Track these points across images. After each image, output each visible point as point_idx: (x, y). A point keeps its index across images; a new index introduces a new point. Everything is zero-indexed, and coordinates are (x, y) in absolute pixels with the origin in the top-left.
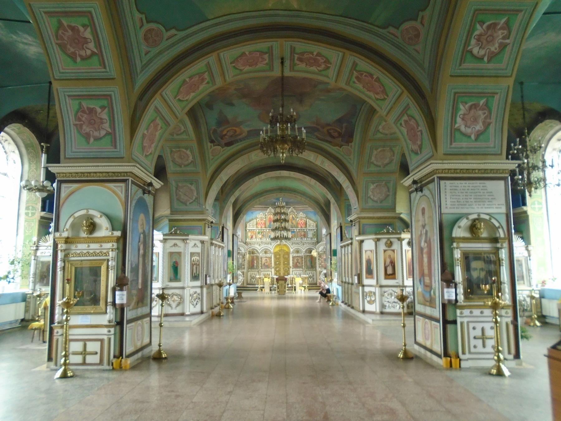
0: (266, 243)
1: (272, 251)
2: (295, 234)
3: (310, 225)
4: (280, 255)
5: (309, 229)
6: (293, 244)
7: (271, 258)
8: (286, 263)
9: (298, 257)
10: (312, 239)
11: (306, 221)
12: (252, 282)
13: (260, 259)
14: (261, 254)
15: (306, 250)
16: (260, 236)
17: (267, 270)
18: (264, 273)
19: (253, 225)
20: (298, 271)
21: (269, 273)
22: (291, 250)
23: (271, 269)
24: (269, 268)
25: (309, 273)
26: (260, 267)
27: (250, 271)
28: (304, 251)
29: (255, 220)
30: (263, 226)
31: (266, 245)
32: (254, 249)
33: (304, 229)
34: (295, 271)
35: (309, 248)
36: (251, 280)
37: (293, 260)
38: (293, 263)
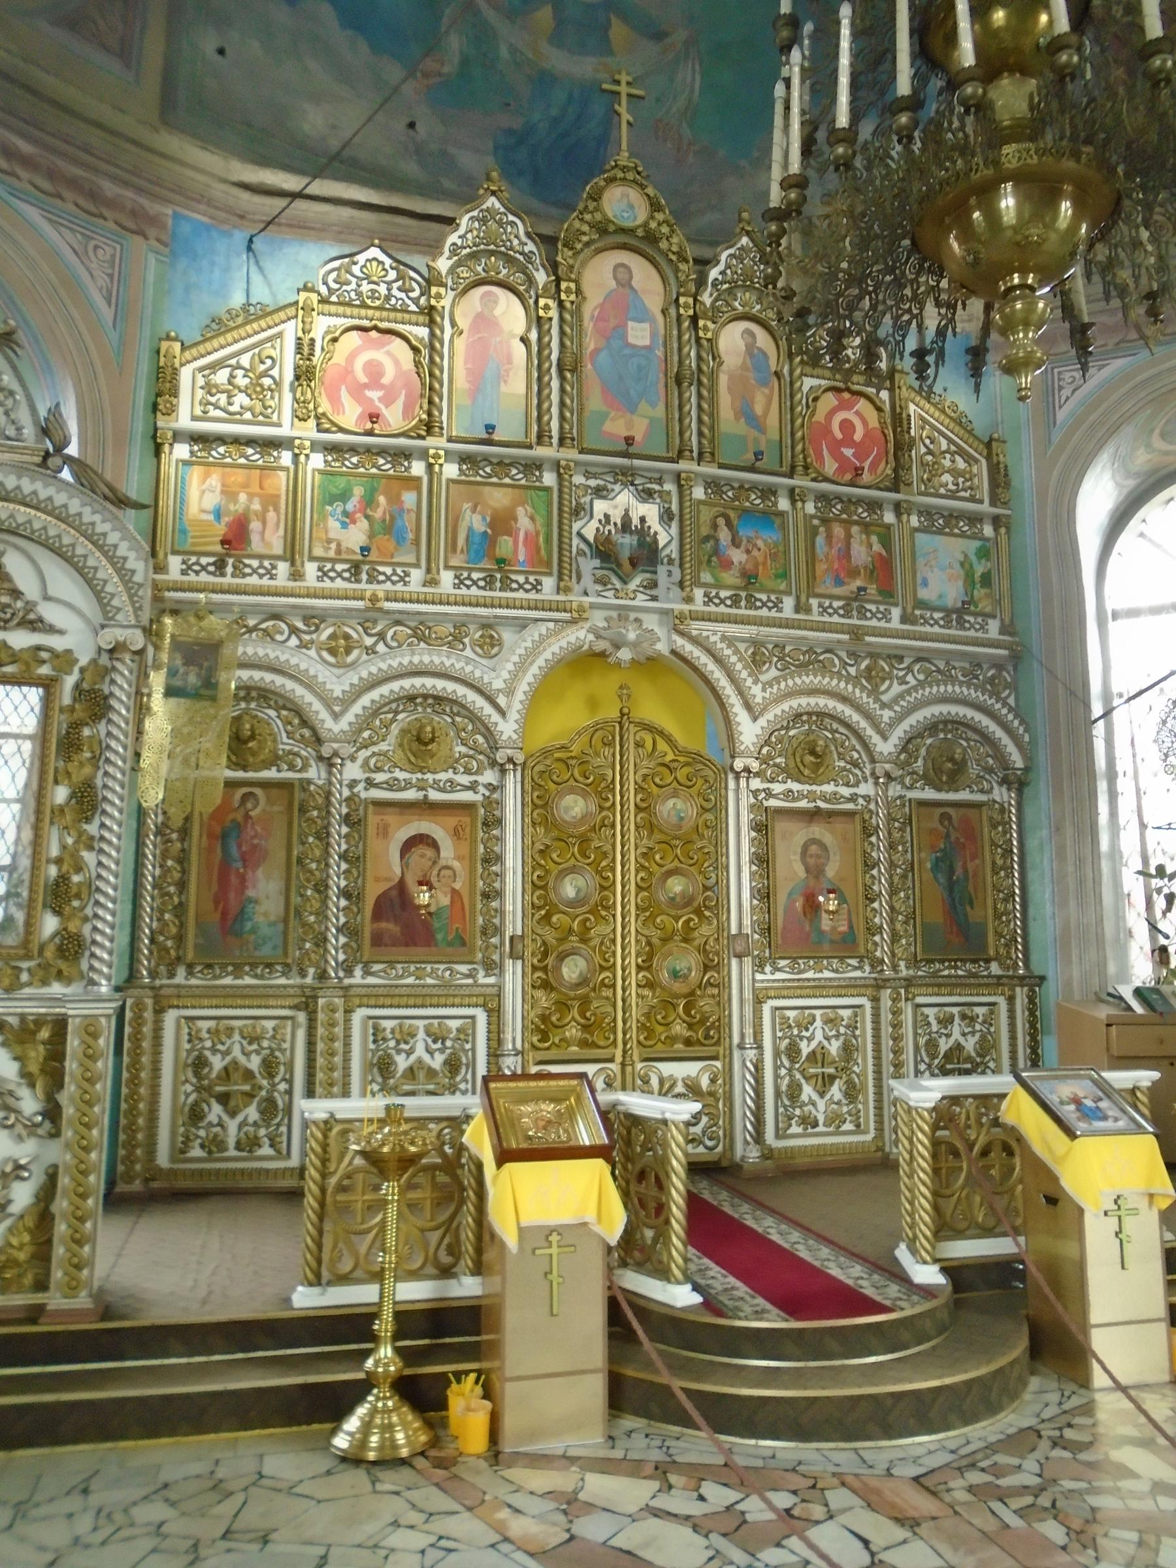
0: (422, 632)
1: (507, 729)
2: (778, 554)
3: (934, 470)
4: (600, 790)
5: (927, 513)
6: (757, 662)
7: (494, 822)
8: (676, 886)
9: (813, 815)
10: (958, 614)
11: (899, 420)
12: (215, 1145)
13: (339, 830)
14: (353, 771)
15: (908, 745)
16: (355, 536)
17: (434, 974)
18: (390, 1018)
19: (255, 390)
20: (819, 988)
21: (453, 1017)
22: (749, 732)
23: (490, 967)
24: (461, 945)
25: (946, 1021)
26: (336, 942)
27: (182, 996)
28: (886, 747)
29: (290, 330)
30: (394, 417)
31: (424, 656)
32: (264, 695)
33: (874, 506)
34: (783, 991)
35: (933, 727)
36: (196, 1115)
37: (763, 860)
38: (765, 895)
